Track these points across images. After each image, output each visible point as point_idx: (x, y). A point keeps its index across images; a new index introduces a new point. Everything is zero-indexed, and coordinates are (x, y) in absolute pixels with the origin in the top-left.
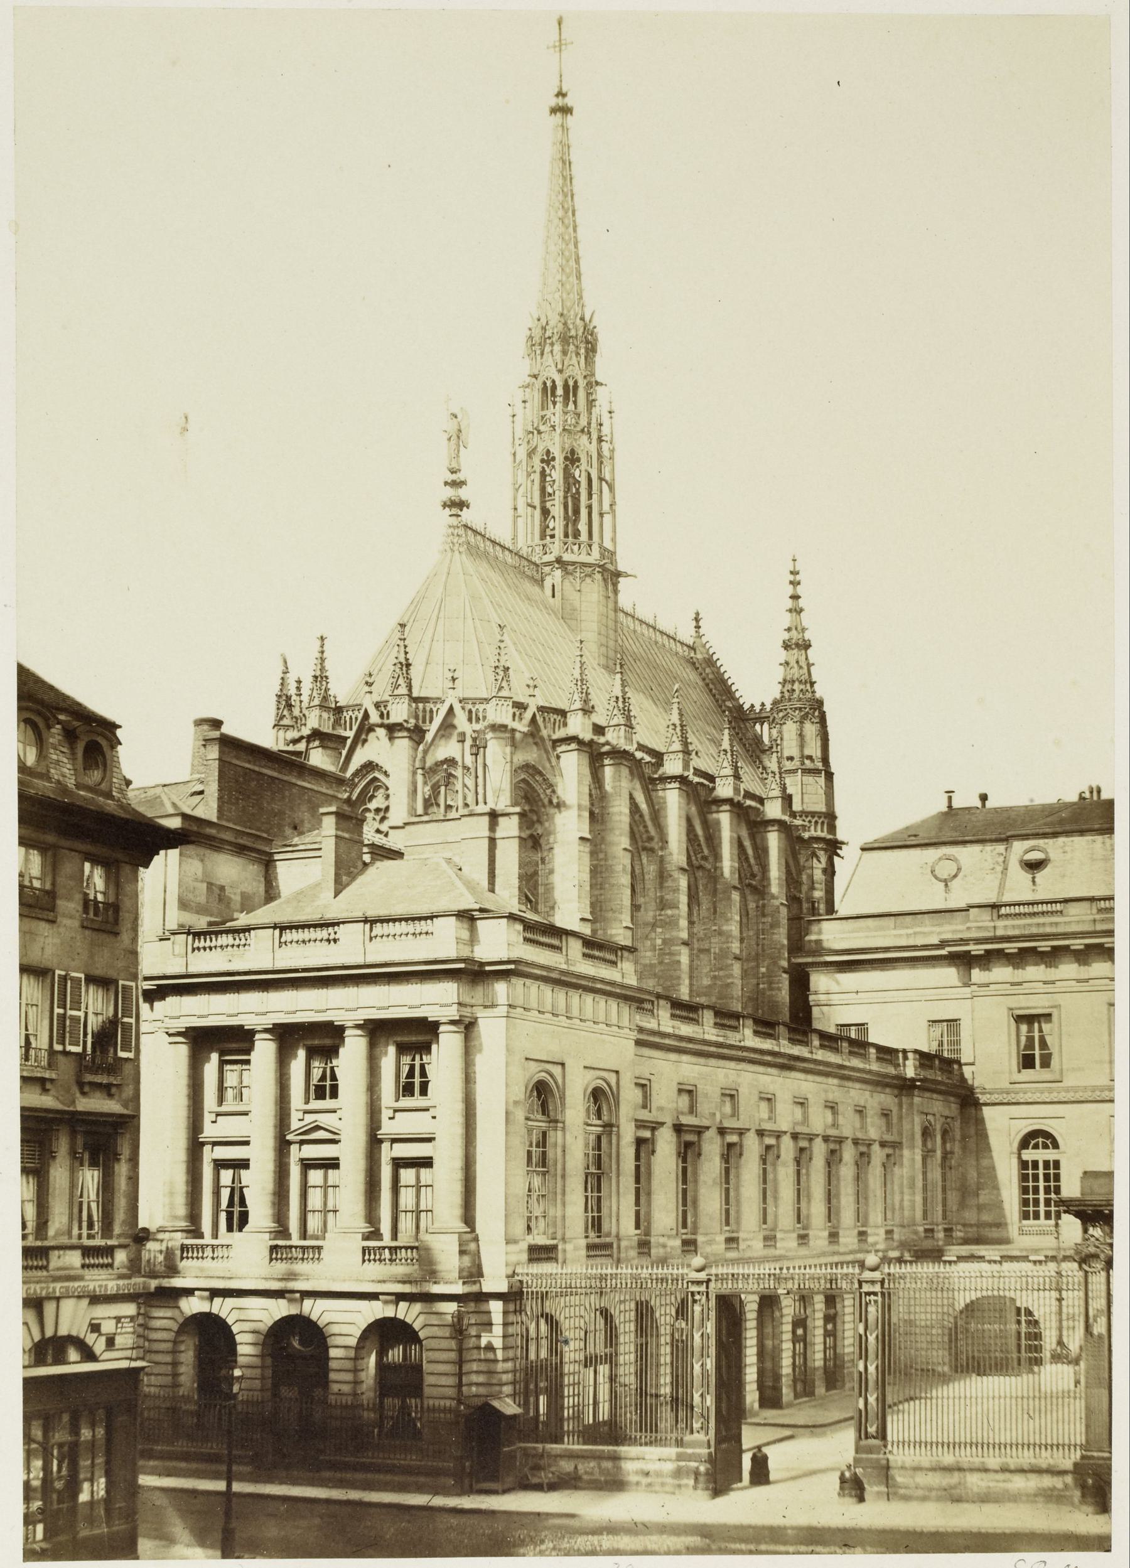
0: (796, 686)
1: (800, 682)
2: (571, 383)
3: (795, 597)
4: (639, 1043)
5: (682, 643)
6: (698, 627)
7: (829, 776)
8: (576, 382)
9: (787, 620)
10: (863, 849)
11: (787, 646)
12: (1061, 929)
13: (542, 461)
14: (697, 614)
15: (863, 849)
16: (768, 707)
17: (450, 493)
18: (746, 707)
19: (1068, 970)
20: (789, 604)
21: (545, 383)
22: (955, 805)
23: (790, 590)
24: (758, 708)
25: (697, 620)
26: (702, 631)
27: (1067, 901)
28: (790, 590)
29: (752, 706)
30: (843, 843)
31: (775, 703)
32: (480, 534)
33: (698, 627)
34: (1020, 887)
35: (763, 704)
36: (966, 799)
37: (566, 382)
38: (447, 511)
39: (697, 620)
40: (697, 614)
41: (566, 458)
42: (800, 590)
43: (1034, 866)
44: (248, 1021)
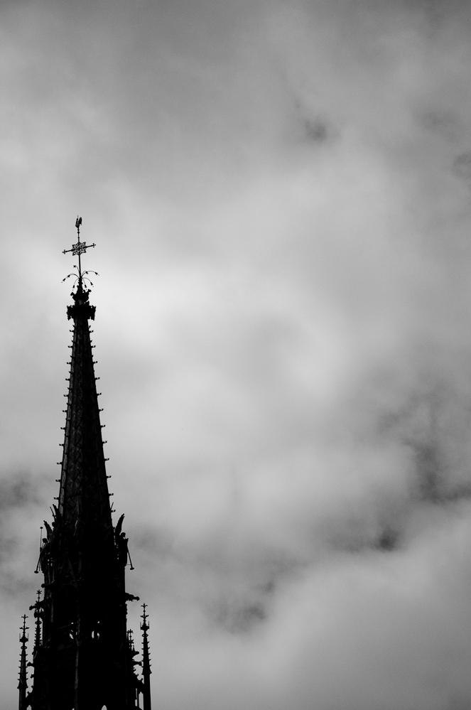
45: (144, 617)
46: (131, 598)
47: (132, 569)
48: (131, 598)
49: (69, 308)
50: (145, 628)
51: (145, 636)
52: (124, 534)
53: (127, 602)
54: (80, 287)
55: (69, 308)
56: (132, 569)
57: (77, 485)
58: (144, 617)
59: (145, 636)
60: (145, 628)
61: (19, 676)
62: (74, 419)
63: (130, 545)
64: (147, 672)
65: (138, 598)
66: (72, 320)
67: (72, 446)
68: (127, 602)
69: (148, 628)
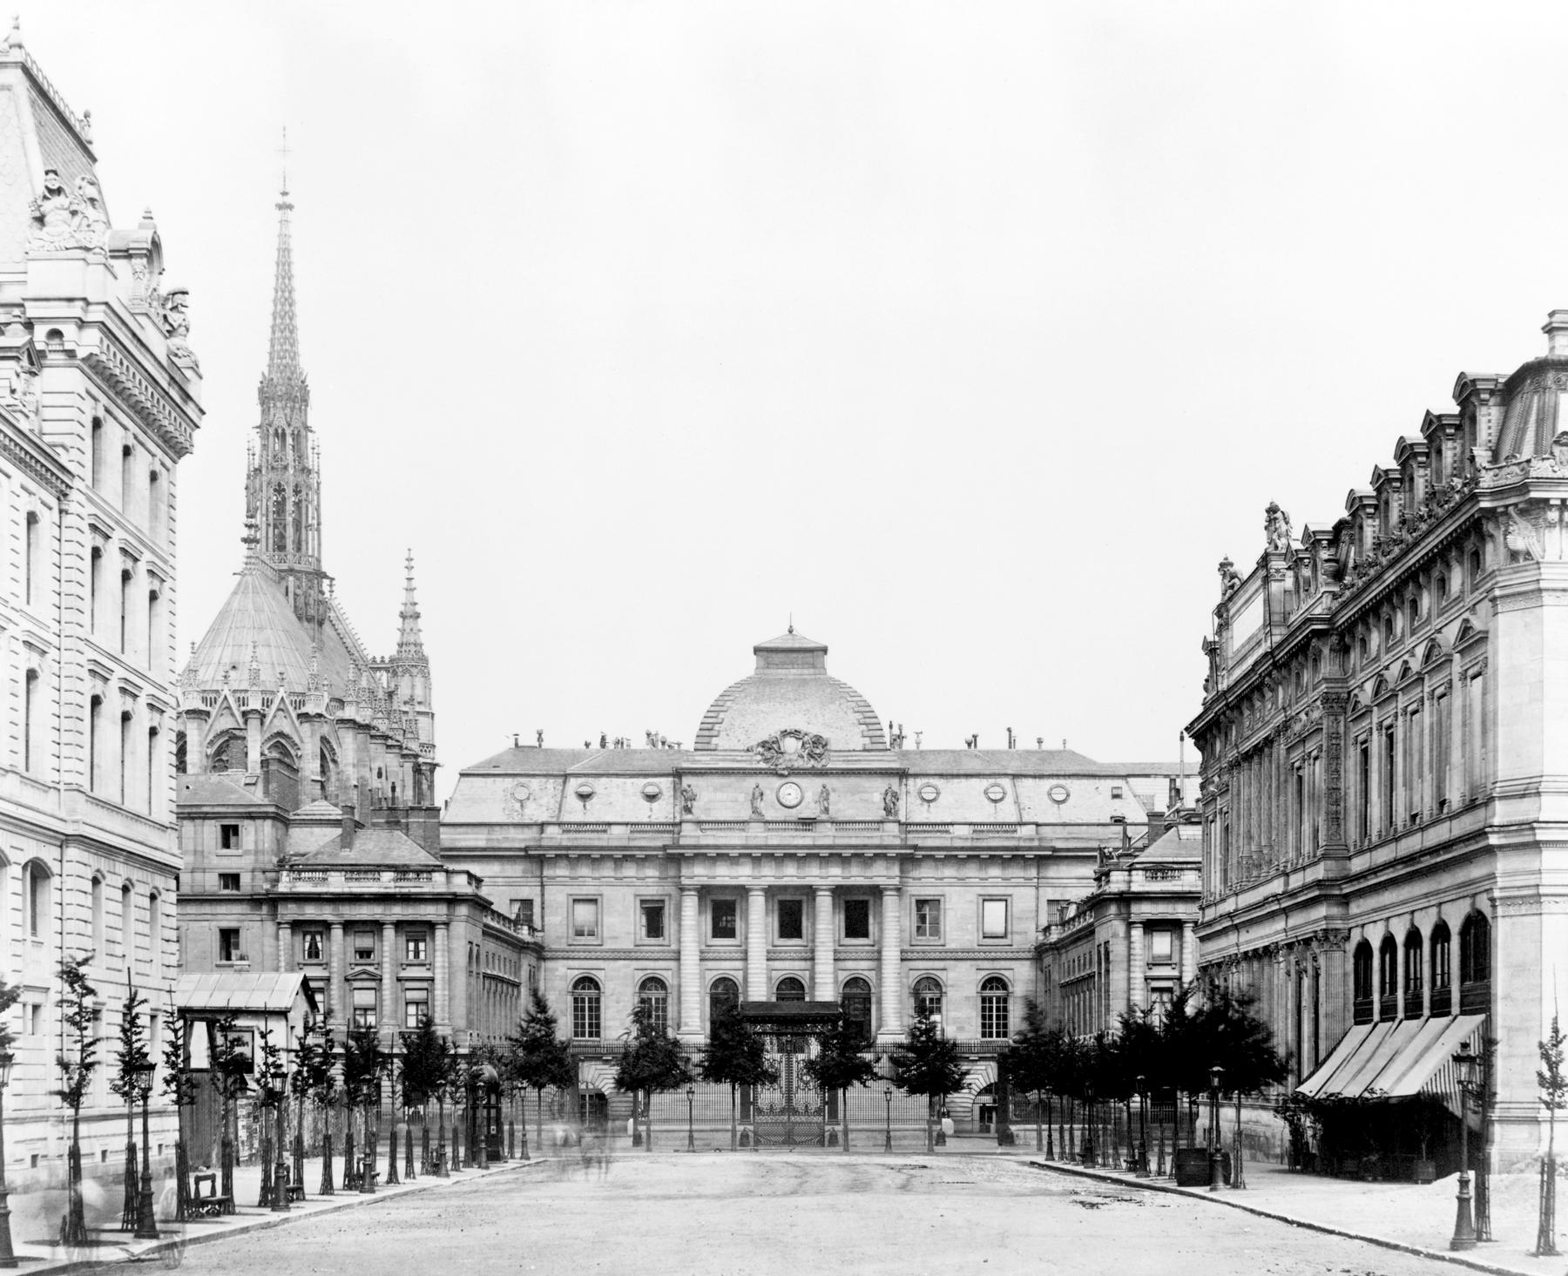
4: (484, 933)
9: (403, 596)
10: (462, 775)
11: (403, 616)
12: (604, 844)
15: (462, 775)
17: (245, 533)
19: (607, 870)
20: (405, 584)
22: (520, 743)
23: (405, 573)
27: (610, 824)
28: (405, 573)
34: (574, 811)
36: (529, 740)
42: (413, 574)
43: (584, 797)
44: (330, 918)
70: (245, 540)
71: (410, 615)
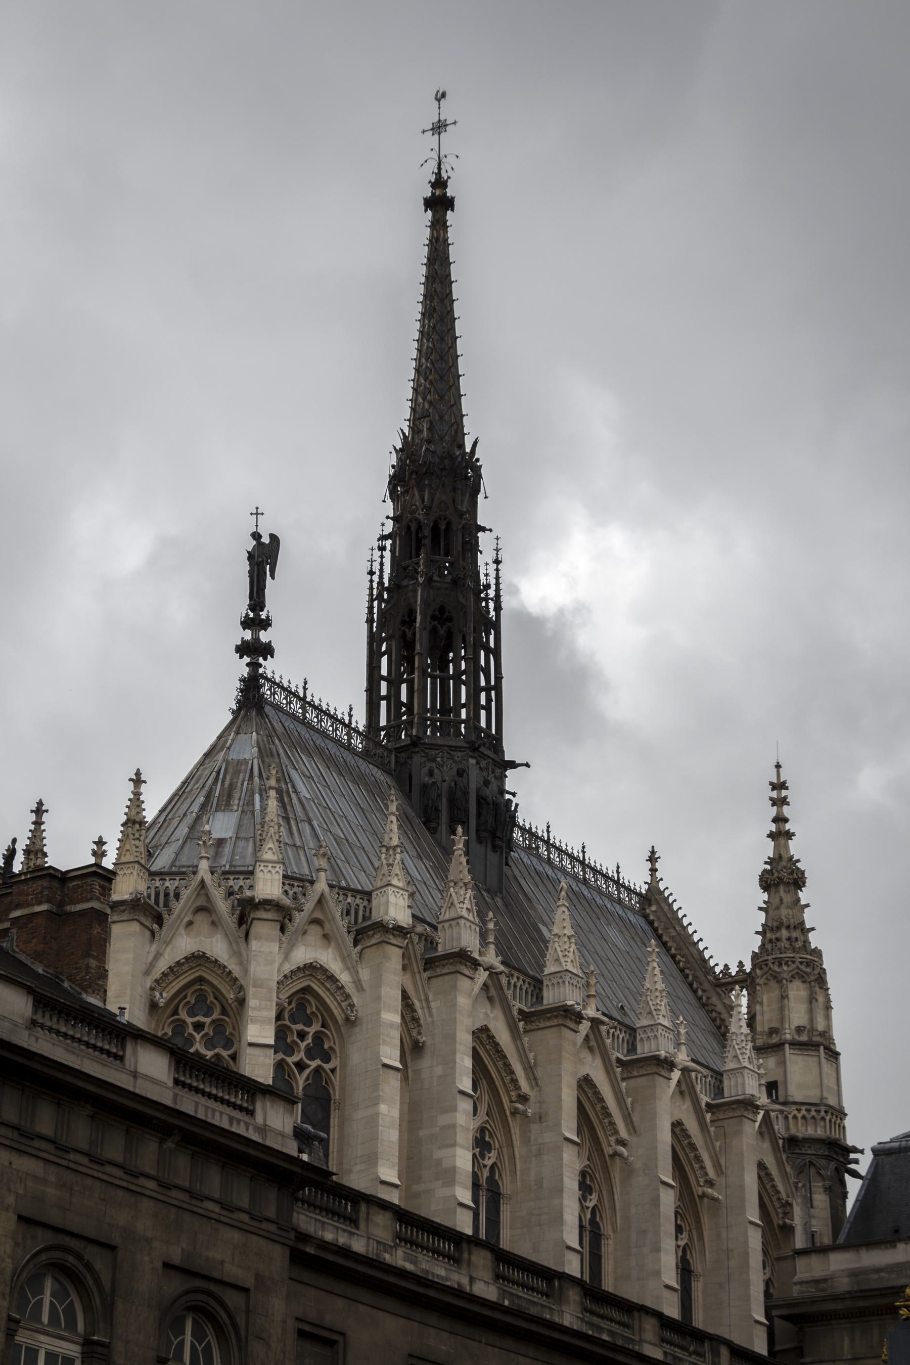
0: (784, 933)
1: (788, 927)
2: (443, 527)
3: (780, 819)
5: (628, 889)
6: (653, 870)
7: (834, 1055)
8: (449, 524)
9: (768, 849)
13: (404, 623)
14: (653, 852)
16: (748, 968)
18: (718, 970)
21: (409, 527)
23: (774, 811)
24: (733, 970)
25: (653, 858)
26: (659, 875)
29: (726, 966)
30: (855, 1150)
31: (755, 956)
32: (295, 695)
33: (653, 870)
35: (741, 964)
37: (436, 523)
38: (247, 659)
39: (653, 858)
40: (653, 852)
41: (433, 618)
45: (497, 550)
46: (483, 529)
47: (486, 497)
48: (483, 529)
49: (425, 200)
50: (497, 562)
51: (497, 570)
52: (478, 460)
53: (480, 534)
54: (439, 174)
55: (425, 200)
56: (486, 497)
57: (427, 406)
58: (497, 550)
59: (497, 570)
60: (497, 562)
61: (366, 611)
62: (426, 330)
63: (483, 471)
64: (498, 608)
65: (491, 530)
66: (429, 212)
67: (423, 360)
68: (480, 534)
69: (501, 562)
70: (243, 649)
71: (782, 878)
